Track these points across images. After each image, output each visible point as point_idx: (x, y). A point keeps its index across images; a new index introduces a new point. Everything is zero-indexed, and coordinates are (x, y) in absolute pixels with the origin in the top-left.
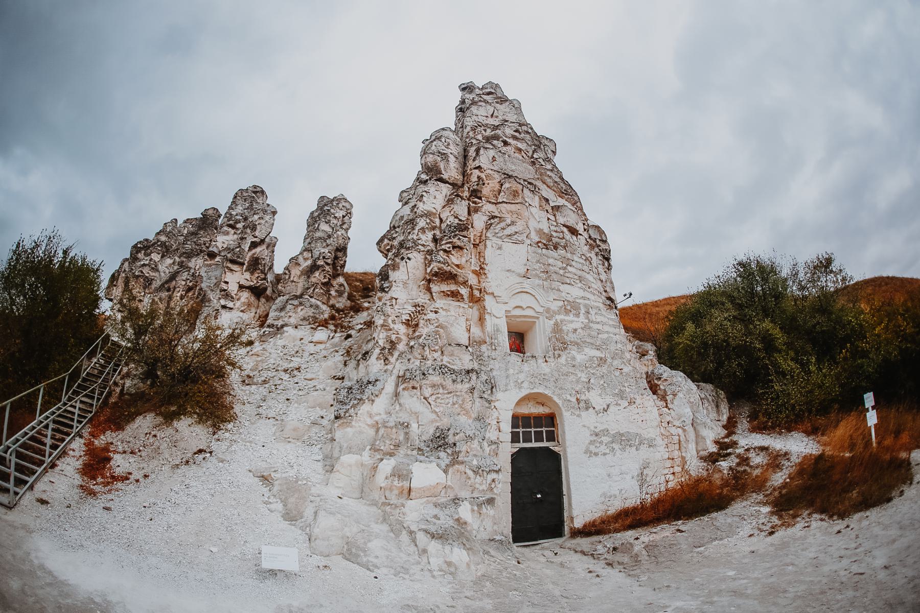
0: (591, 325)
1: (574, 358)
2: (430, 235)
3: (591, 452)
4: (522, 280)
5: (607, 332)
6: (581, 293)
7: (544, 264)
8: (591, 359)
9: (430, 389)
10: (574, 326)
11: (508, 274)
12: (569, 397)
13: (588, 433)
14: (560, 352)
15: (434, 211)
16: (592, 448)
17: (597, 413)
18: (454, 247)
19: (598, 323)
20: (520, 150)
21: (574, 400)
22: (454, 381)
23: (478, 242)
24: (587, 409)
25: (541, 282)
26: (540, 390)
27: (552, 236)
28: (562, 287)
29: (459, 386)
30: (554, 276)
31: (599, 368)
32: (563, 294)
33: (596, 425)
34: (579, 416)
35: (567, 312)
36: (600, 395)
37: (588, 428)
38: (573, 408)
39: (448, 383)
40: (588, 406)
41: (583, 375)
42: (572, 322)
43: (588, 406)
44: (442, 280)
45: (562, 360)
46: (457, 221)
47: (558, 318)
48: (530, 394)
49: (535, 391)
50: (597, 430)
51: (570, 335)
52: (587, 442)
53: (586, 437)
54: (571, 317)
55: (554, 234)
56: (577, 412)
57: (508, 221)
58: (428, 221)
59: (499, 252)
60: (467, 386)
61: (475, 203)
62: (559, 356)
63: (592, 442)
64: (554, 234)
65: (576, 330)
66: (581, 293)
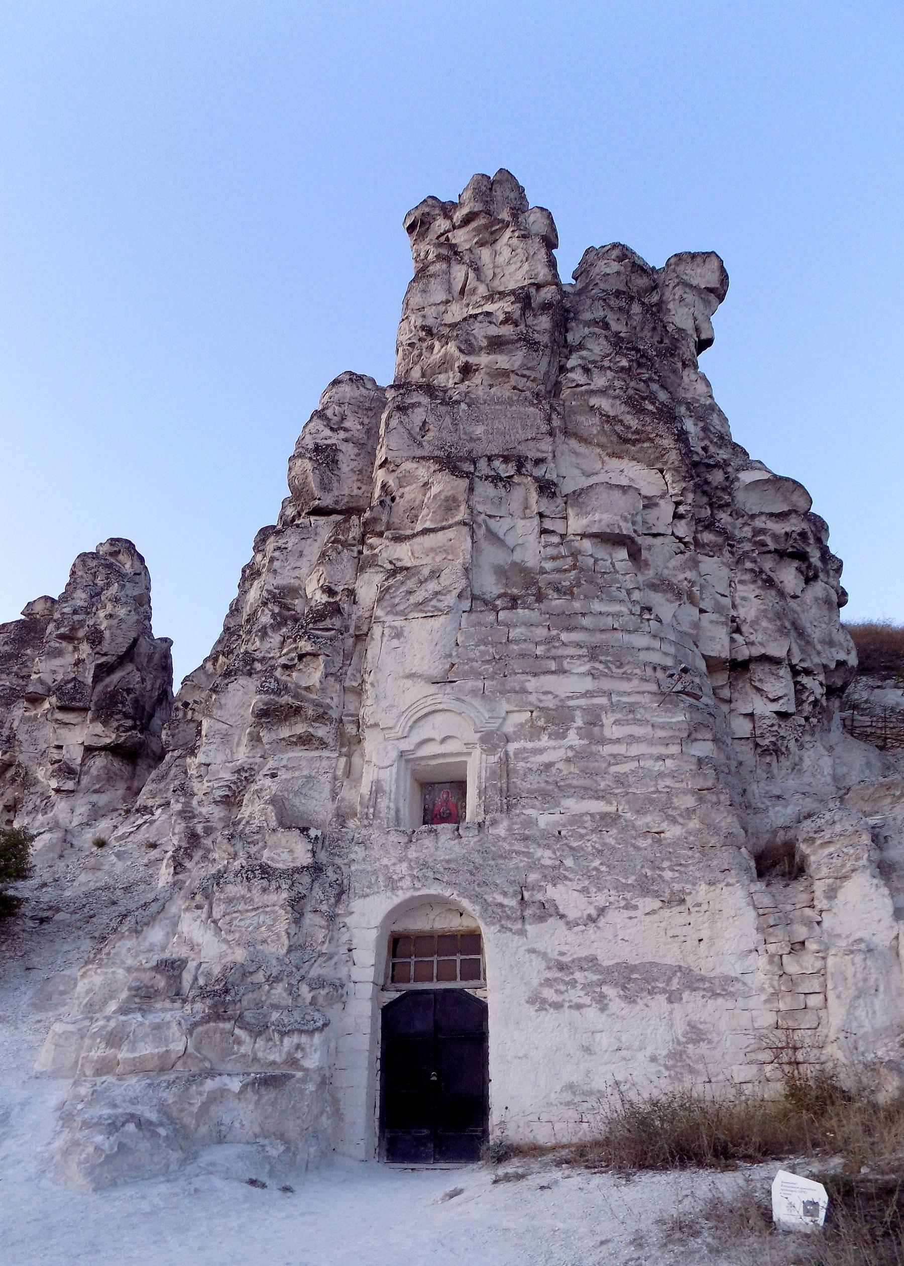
0: (594, 748)
1: (530, 823)
2: (275, 638)
3: (544, 1001)
4: (434, 688)
5: (638, 758)
6: (588, 684)
7: (494, 644)
8: (576, 820)
9: (223, 906)
10: (545, 758)
11: (408, 683)
12: (500, 899)
13: (538, 963)
14: (497, 815)
15: (296, 583)
16: (548, 994)
17: (571, 925)
18: (301, 657)
19: (618, 741)
20: (505, 374)
21: (512, 902)
22: (264, 890)
23: (365, 628)
24: (542, 919)
25: (480, 684)
26: (434, 890)
27: (543, 571)
28: (532, 684)
29: (272, 898)
30: (515, 665)
31: (594, 837)
32: (532, 698)
33: (564, 948)
34: (522, 933)
35: (535, 732)
36: (584, 890)
37: (545, 955)
38: (508, 918)
39: (256, 893)
40: (547, 911)
41: (548, 853)
42: (541, 751)
43: (547, 911)
44: (280, 721)
45: (501, 830)
46: (325, 598)
47: (512, 747)
48: (413, 899)
49: (424, 891)
50: (564, 959)
51: (530, 778)
52: (535, 982)
53: (535, 970)
54: (544, 741)
55: (549, 565)
56: (518, 926)
57: (426, 572)
58: (277, 610)
59: (395, 643)
60: (285, 895)
61: (372, 547)
62: (494, 823)
63: (548, 983)
64: (549, 565)
65: (549, 765)
66: (588, 684)
